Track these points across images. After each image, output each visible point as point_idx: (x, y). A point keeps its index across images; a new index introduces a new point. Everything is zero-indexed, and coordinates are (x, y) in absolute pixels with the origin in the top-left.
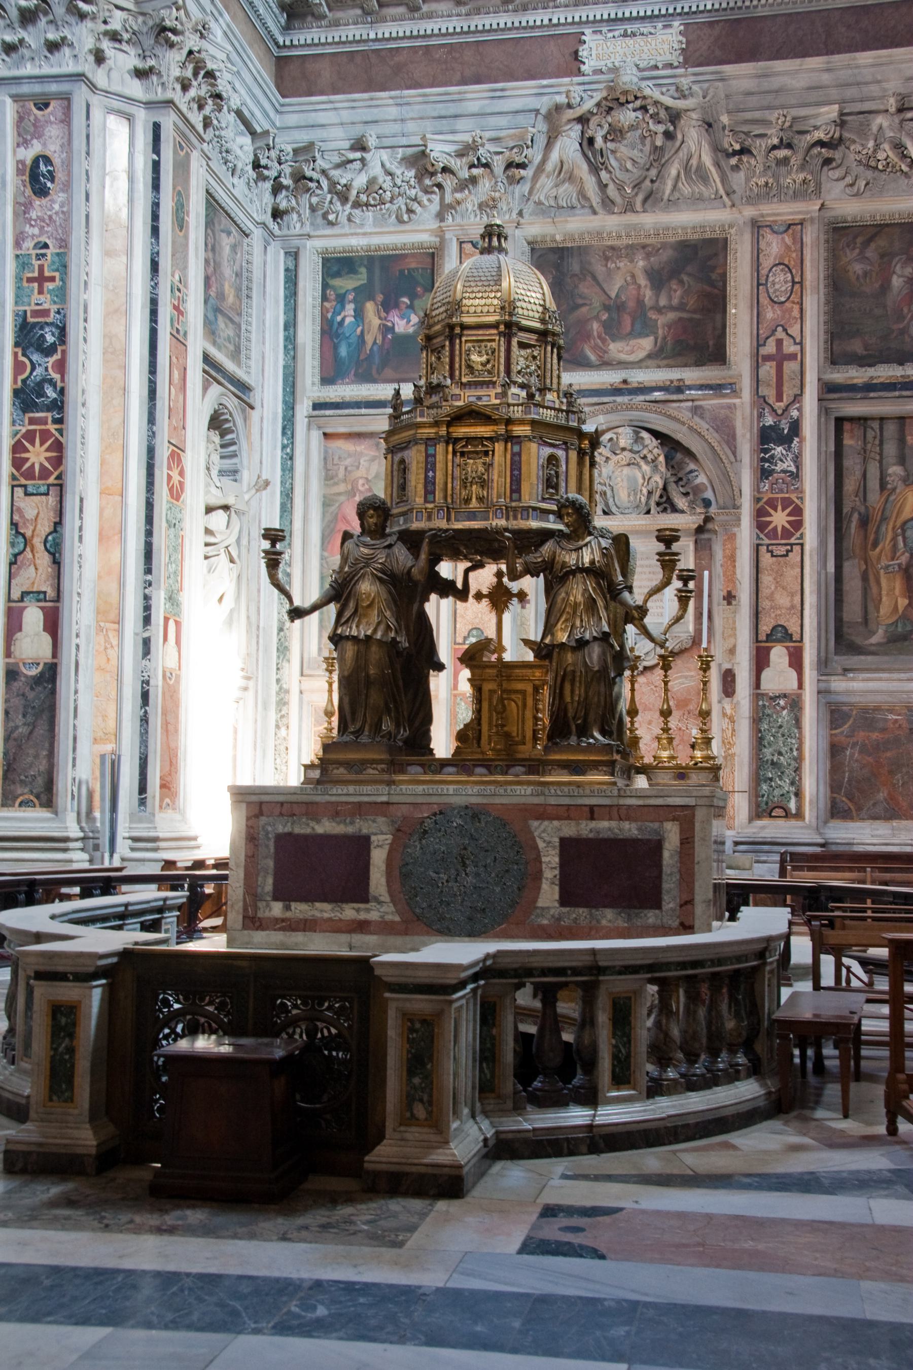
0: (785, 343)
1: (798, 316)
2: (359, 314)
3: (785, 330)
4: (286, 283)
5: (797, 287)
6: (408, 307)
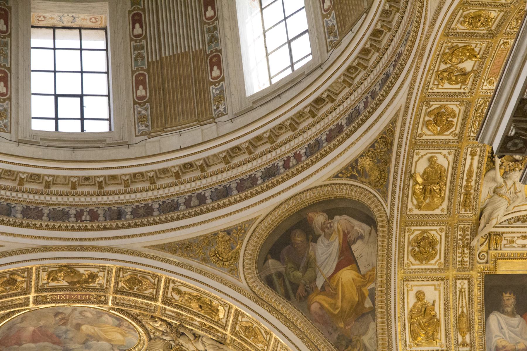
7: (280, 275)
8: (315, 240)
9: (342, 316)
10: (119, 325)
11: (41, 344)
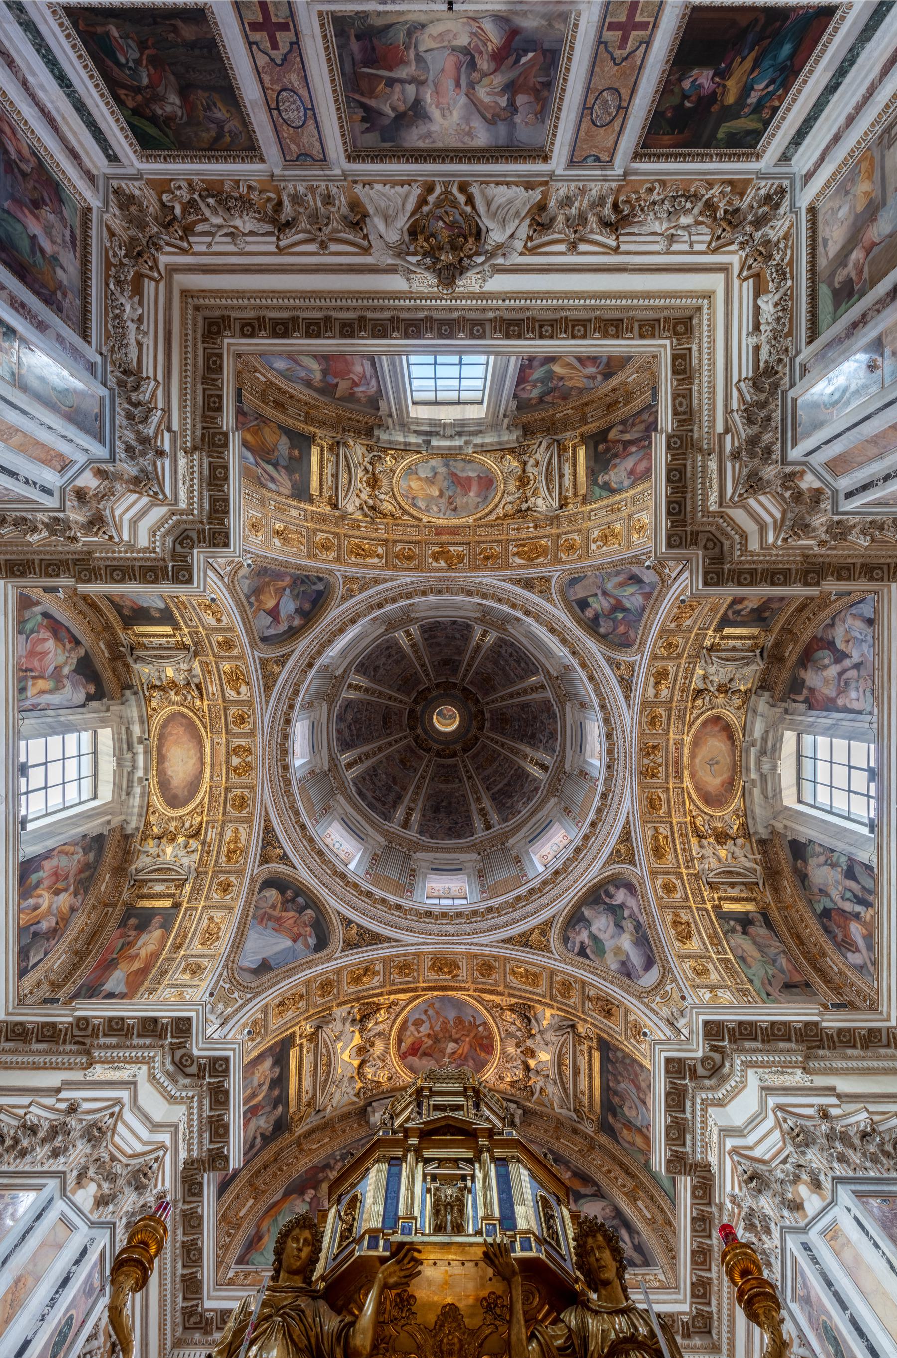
0: (268, 45)
1: (262, 75)
2: (746, 90)
3: (272, 60)
4: (807, 133)
5: (273, 105)
6: (685, 97)
7: (315, 584)
8: (296, 611)
9: (268, 584)
10: (414, 498)
11: (464, 475)
